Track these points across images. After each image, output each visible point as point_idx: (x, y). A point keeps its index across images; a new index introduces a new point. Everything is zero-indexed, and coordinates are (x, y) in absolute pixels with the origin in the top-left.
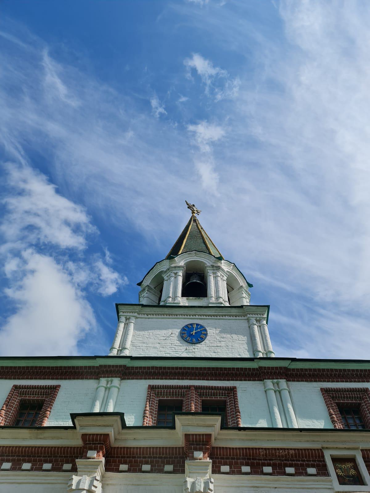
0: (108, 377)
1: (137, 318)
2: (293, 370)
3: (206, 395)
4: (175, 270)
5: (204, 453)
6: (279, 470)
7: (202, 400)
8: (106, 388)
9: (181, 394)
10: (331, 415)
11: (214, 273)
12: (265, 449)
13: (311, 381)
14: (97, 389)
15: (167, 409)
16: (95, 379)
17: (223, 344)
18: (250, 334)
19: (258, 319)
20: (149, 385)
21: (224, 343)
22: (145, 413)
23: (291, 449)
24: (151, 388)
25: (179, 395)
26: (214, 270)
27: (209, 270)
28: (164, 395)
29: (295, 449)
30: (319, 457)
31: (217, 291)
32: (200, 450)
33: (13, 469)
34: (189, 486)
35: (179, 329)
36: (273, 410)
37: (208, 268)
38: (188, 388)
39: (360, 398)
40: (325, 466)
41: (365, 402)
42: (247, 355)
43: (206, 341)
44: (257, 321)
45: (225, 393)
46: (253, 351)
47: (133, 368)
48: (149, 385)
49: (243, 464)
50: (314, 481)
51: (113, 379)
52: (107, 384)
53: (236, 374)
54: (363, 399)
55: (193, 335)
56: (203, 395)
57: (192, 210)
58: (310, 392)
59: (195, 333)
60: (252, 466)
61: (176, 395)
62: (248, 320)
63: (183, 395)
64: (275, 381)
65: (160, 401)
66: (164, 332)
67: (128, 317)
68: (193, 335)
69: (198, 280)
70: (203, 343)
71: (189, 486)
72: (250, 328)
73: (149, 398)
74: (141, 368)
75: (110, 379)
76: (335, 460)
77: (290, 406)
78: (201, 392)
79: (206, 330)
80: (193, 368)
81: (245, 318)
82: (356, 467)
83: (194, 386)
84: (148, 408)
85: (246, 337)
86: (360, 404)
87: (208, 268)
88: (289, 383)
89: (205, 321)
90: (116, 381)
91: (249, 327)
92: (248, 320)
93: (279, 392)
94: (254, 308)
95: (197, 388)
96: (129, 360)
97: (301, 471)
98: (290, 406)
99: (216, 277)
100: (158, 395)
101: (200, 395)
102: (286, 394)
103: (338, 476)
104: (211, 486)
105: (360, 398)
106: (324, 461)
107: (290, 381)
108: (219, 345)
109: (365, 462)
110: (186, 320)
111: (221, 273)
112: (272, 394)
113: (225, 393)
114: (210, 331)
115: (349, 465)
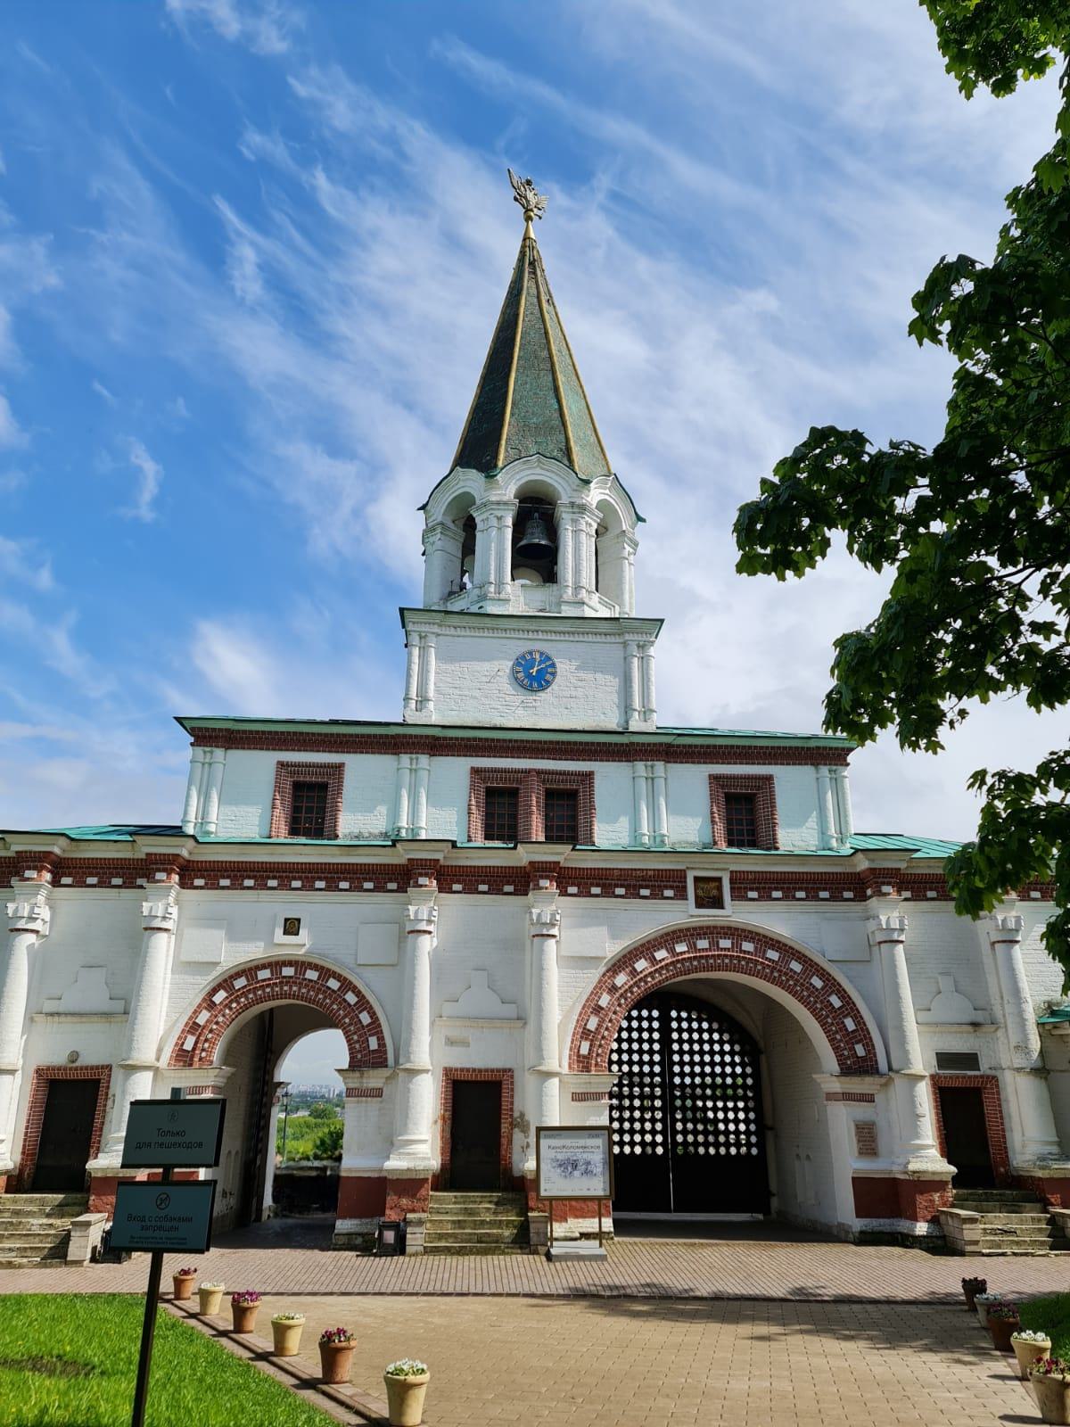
0: (411, 753)
5: (551, 881)
6: (632, 893)
8: (411, 770)
10: (712, 813)
11: (575, 521)
13: (699, 763)
14: (398, 769)
15: (499, 807)
16: (392, 754)
17: (580, 692)
18: (625, 672)
20: (472, 768)
21: (578, 702)
22: (470, 809)
26: (574, 513)
29: (654, 870)
31: (577, 571)
32: (547, 877)
34: (535, 918)
35: (510, 660)
36: (639, 806)
37: (563, 509)
38: (528, 772)
40: (685, 888)
42: (613, 726)
43: (554, 686)
44: (639, 646)
46: (626, 707)
48: (472, 768)
49: (592, 885)
52: (411, 764)
53: (596, 751)
55: (534, 676)
57: (523, 206)
58: (694, 779)
59: (537, 671)
62: (625, 644)
63: (519, 781)
64: (649, 763)
66: (486, 666)
68: (534, 676)
69: (543, 539)
70: (548, 690)
71: (535, 918)
72: (626, 660)
73: (473, 787)
74: (457, 739)
75: (414, 756)
77: (662, 802)
79: (553, 665)
80: (533, 742)
81: (621, 641)
82: (720, 888)
83: (535, 770)
84: (473, 803)
85: (617, 680)
87: (563, 509)
88: (669, 765)
89: (554, 644)
90: (424, 759)
91: (625, 658)
92: (625, 644)
93: (652, 780)
94: (637, 624)
95: (539, 772)
97: (657, 895)
98: (662, 802)
99: (576, 532)
100: (484, 780)
101: (544, 782)
102: (660, 783)
103: (697, 897)
104: (558, 917)
106: (685, 882)
107: (669, 762)
108: (574, 694)
109: (731, 883)
110: (520, 643)
111: (587, 519)
112: (642, 784)
114: (563, 666)
115: (714, 884)
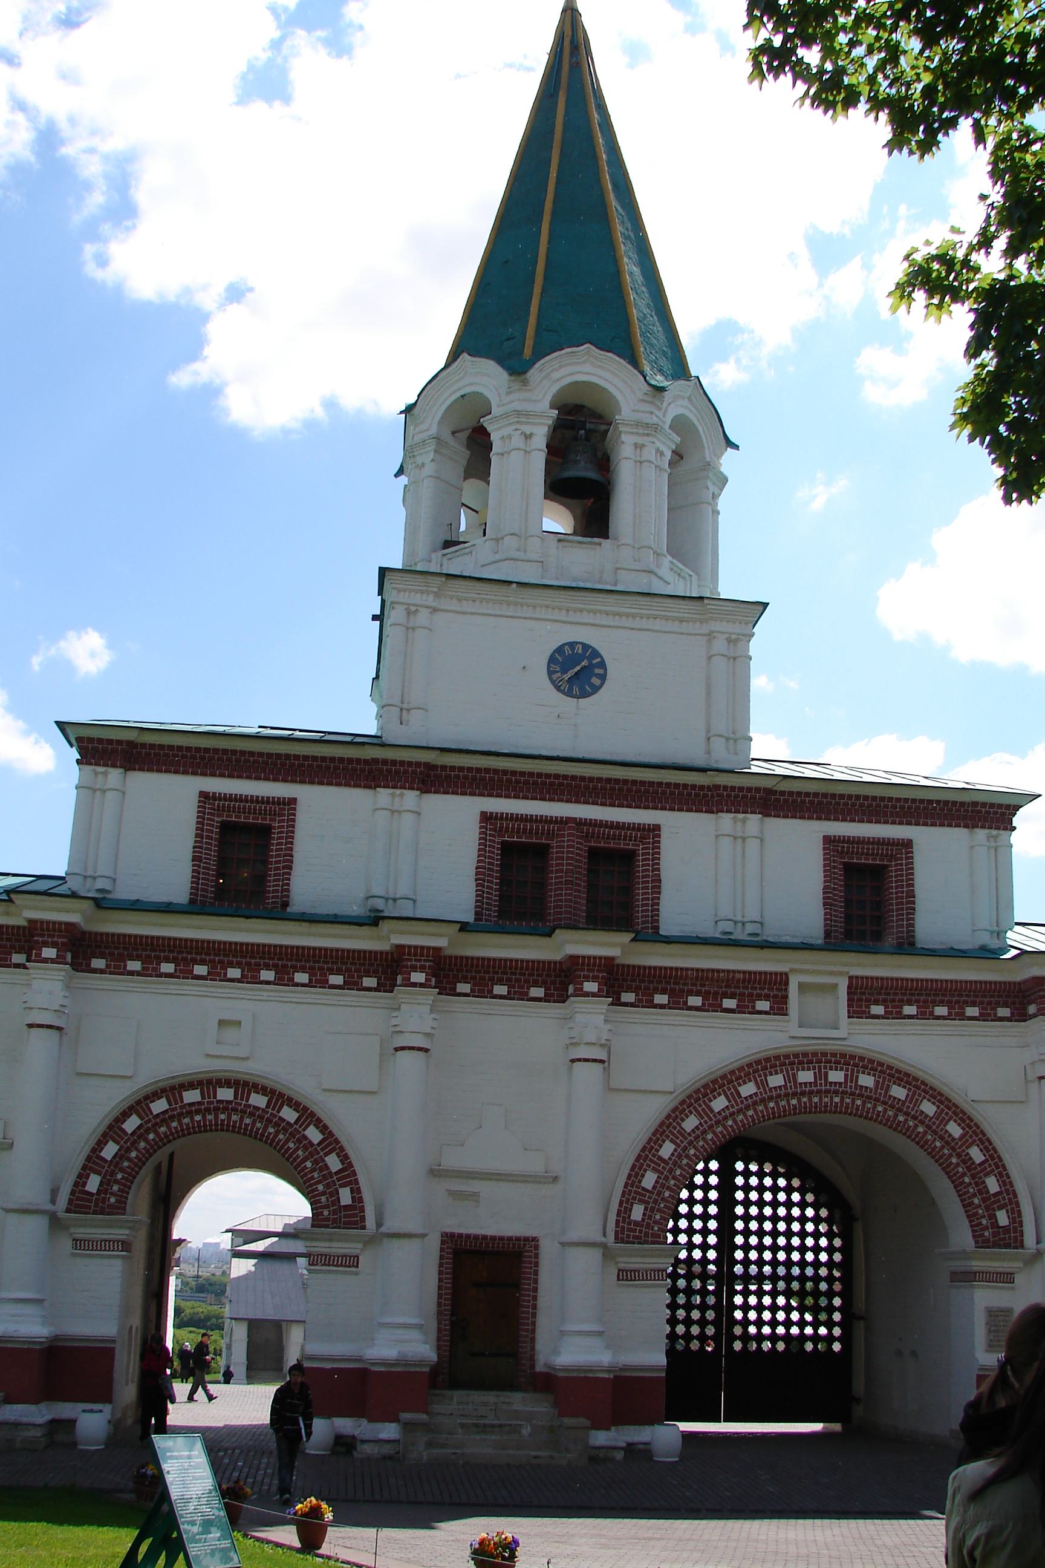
1: (435, 610)
2: (782, 793)
3: (598, 837)
4: (527, 423)
7: (590, 848)
9: (548, 834)
12: (697, 970)
13: (810, 818)
19: (733, 637)
23: (739, 972)
24: (487, 818)
25: (543, 834)
27: (626, 433)
28: (513, 831)
30: (780, 984)
33: (278, 982)
39: (892, 855)
41: (896, 865)
45: (636, 837)
47: (444, 767)
50: (762, 1020)
51: (405, 791)
54: (897, 859)
56: (592, 837)
60: (672, 994)
61: (537, 833)
63: (550, 835)
65: (503, 843)
67: (413, 608)
76: (802, 987)
78: (588, 833)
86: (887, 866)
95: (581, 823)
96: (438, 752)
105: (892, 855)
113: (636, 837)
